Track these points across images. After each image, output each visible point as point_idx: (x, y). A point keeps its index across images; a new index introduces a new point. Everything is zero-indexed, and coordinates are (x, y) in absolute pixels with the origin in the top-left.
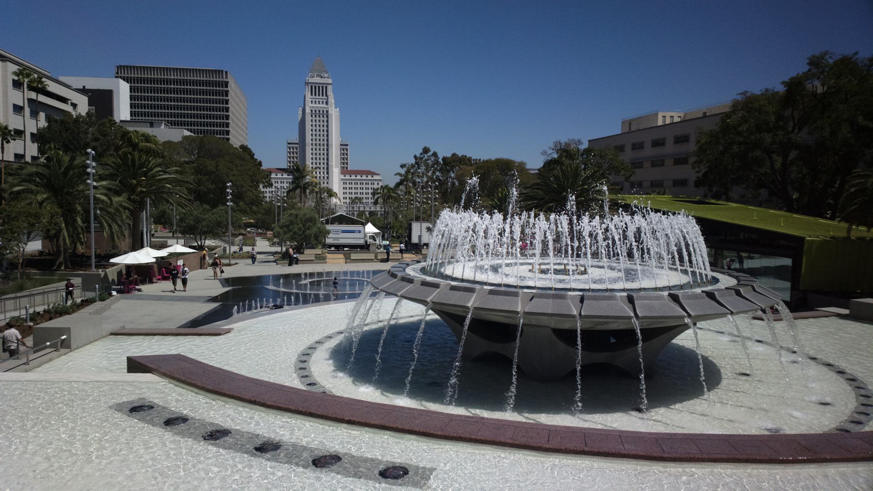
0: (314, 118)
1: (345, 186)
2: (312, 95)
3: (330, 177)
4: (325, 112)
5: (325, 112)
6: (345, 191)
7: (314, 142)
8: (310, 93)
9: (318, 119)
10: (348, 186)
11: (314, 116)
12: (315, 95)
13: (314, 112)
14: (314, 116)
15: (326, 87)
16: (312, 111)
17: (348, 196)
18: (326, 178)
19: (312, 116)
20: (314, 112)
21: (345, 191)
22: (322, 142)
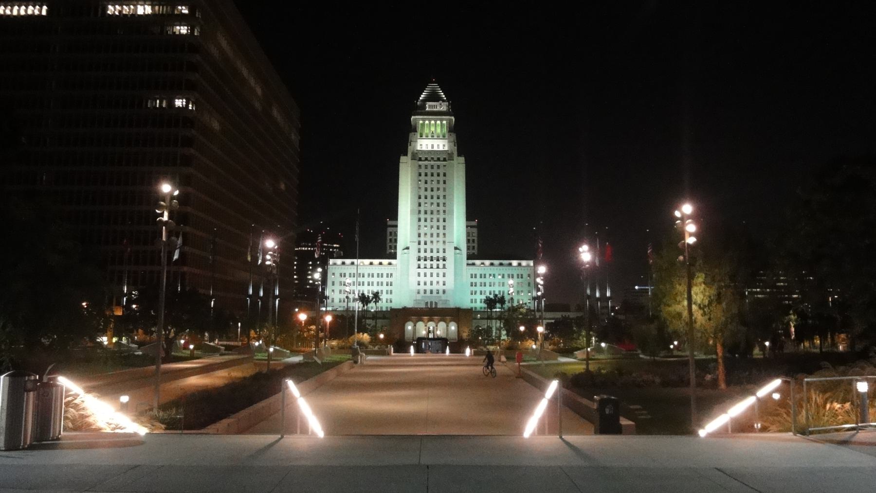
1: (474, 280)
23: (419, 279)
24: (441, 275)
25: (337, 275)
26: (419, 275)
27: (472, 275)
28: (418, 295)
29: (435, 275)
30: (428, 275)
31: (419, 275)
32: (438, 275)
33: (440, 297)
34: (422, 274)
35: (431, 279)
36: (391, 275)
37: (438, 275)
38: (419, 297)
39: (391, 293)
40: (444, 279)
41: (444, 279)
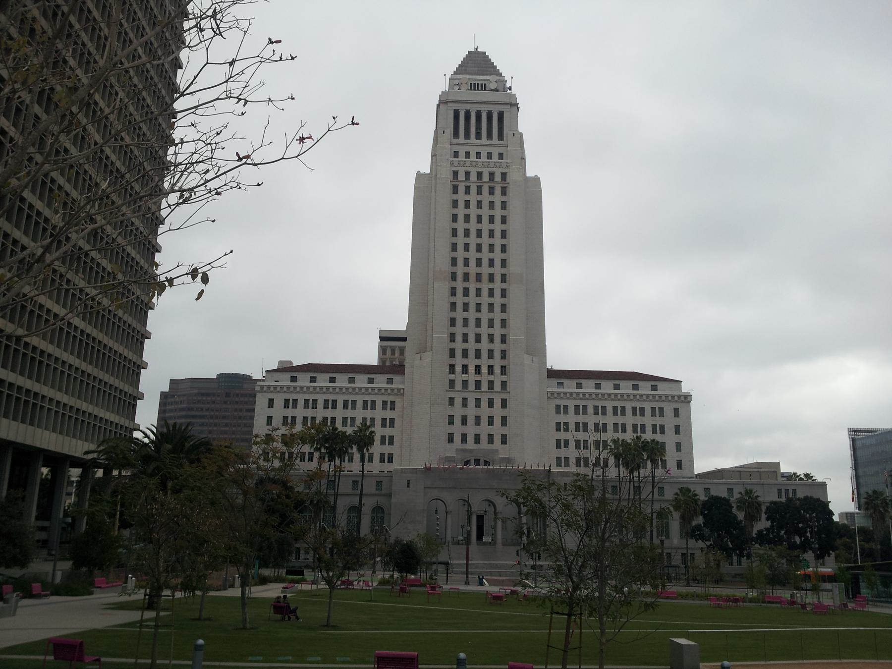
0: (461, 197)
1: (562, 418)
2: (456, 134)
3: (510, 386)
4: (498, 178)
5: (498, 178)
6: (562, 436)
7: (460, 269)
8: (450, 130)
9: (473, 197)
10: (572, 418)
11: (461, 189)
12: (467, 136)
13: (462, 176)
14: (461, 189)
15: (501, 116)
16: (455, 174)
17: (572, 453)
18: (497, 387)
19: (455, 190)
20: (462, 176)
21: (562, 436)
22: (485, 270)
23: (450, 411)
24: (498, 403)
25: (279, 403)
26: (451, 401)
27: (558, 407)
28: (449, 446)
29: (484, 404)
30: (471, 403)
31: (451, 401)
32: (491, 404)
33: (497, 451)
34: (458, 402)
35: (478, 412)
36: (393, 403)
37: (491, 404)
38: (451, 451)
39: (391, 442)
40: (504, 413)
41: (504, 413)
